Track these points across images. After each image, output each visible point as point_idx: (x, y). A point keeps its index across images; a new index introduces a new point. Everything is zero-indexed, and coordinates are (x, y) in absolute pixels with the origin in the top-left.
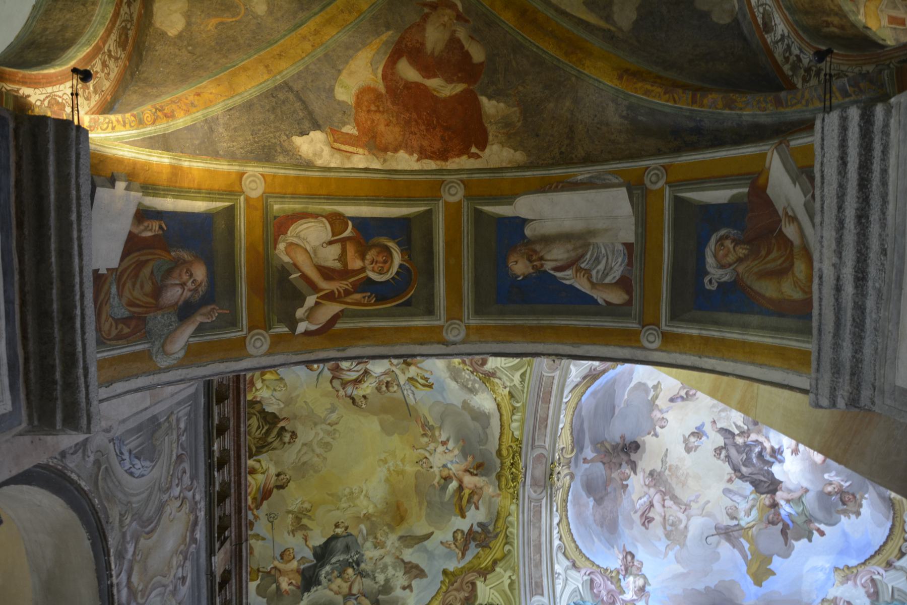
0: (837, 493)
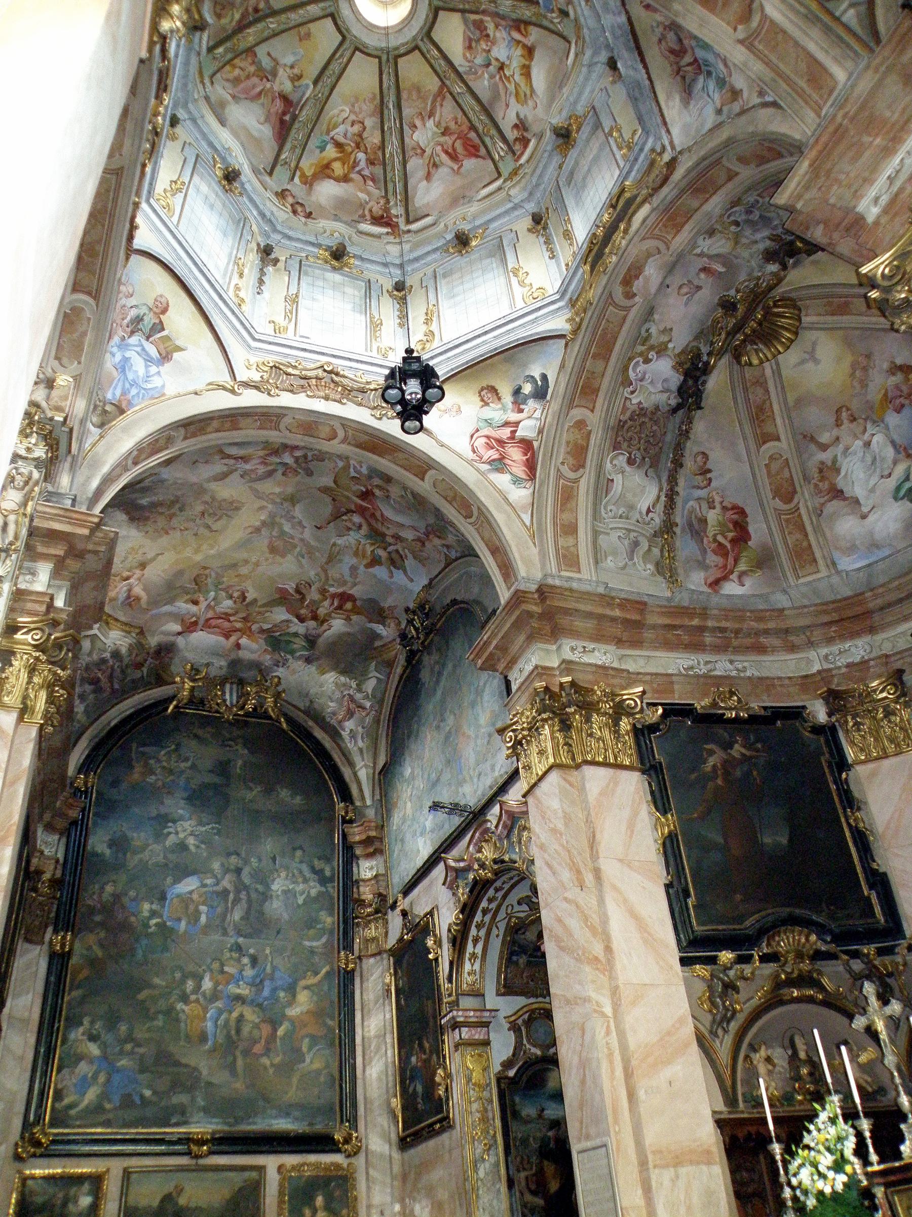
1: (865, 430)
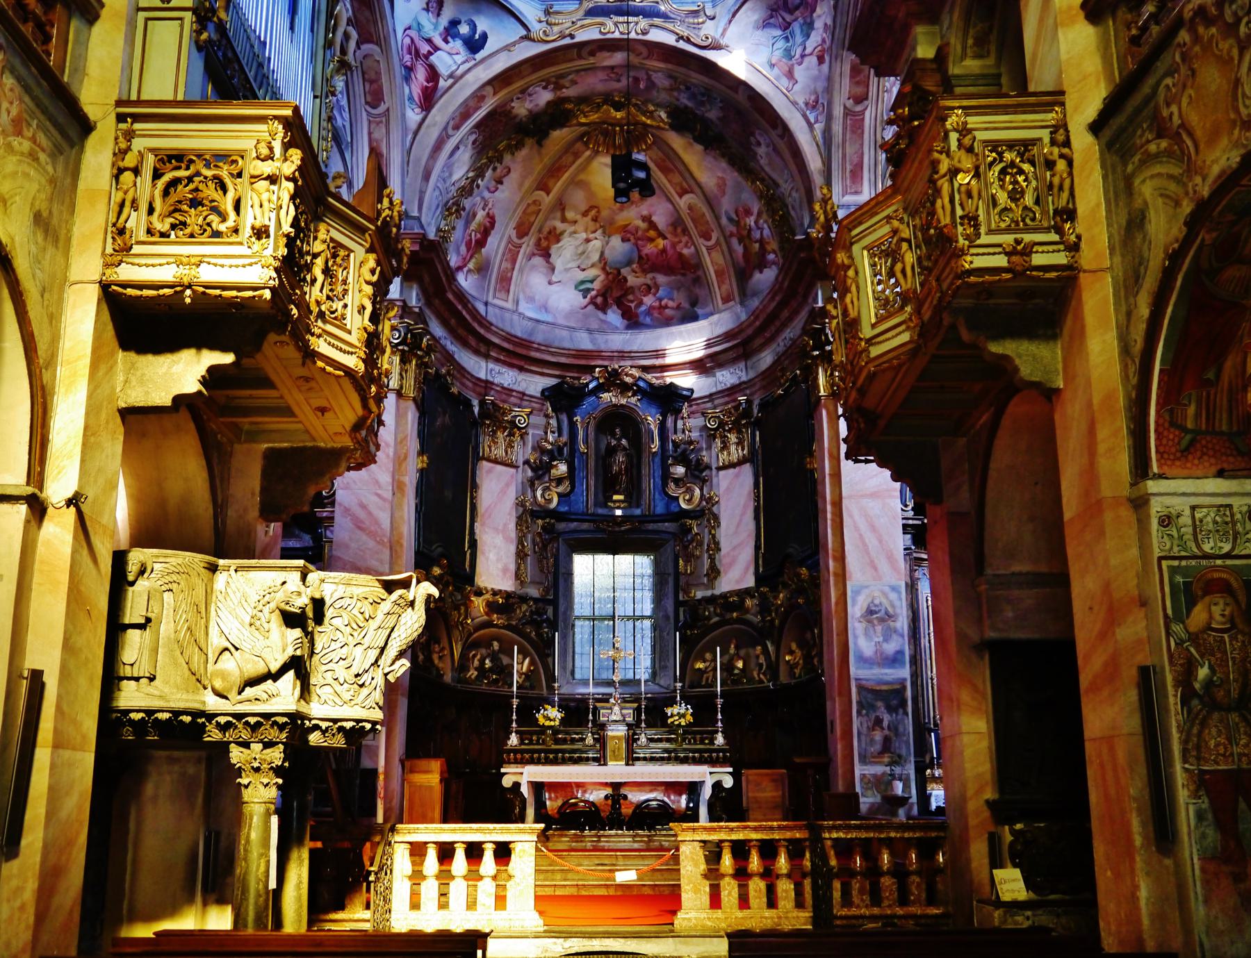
1: (594, 232)
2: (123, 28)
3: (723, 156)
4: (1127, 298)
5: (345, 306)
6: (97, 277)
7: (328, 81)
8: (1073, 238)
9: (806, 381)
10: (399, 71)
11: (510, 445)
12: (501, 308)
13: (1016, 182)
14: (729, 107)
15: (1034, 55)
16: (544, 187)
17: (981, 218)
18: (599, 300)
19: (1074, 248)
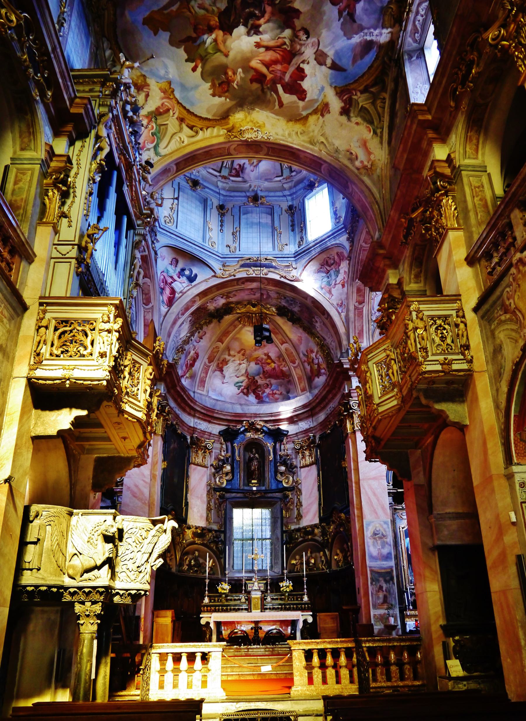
0: (227, 78)
2: (44, 266)
3: (301, 327)
4: (496, 384)
5: (138, 389)
6: (26, 375)
7: (130, 292)
8: (469, 357)
9: (341, 426)
10: (158, 290)
11: (204, 457)
12: (201, 394)
13: (442, 333)
14: (303, 306)
15: (445, 280)
16: (221, 340)
17: (428, 349)
18: (245, 391)
19: (470, 362)
